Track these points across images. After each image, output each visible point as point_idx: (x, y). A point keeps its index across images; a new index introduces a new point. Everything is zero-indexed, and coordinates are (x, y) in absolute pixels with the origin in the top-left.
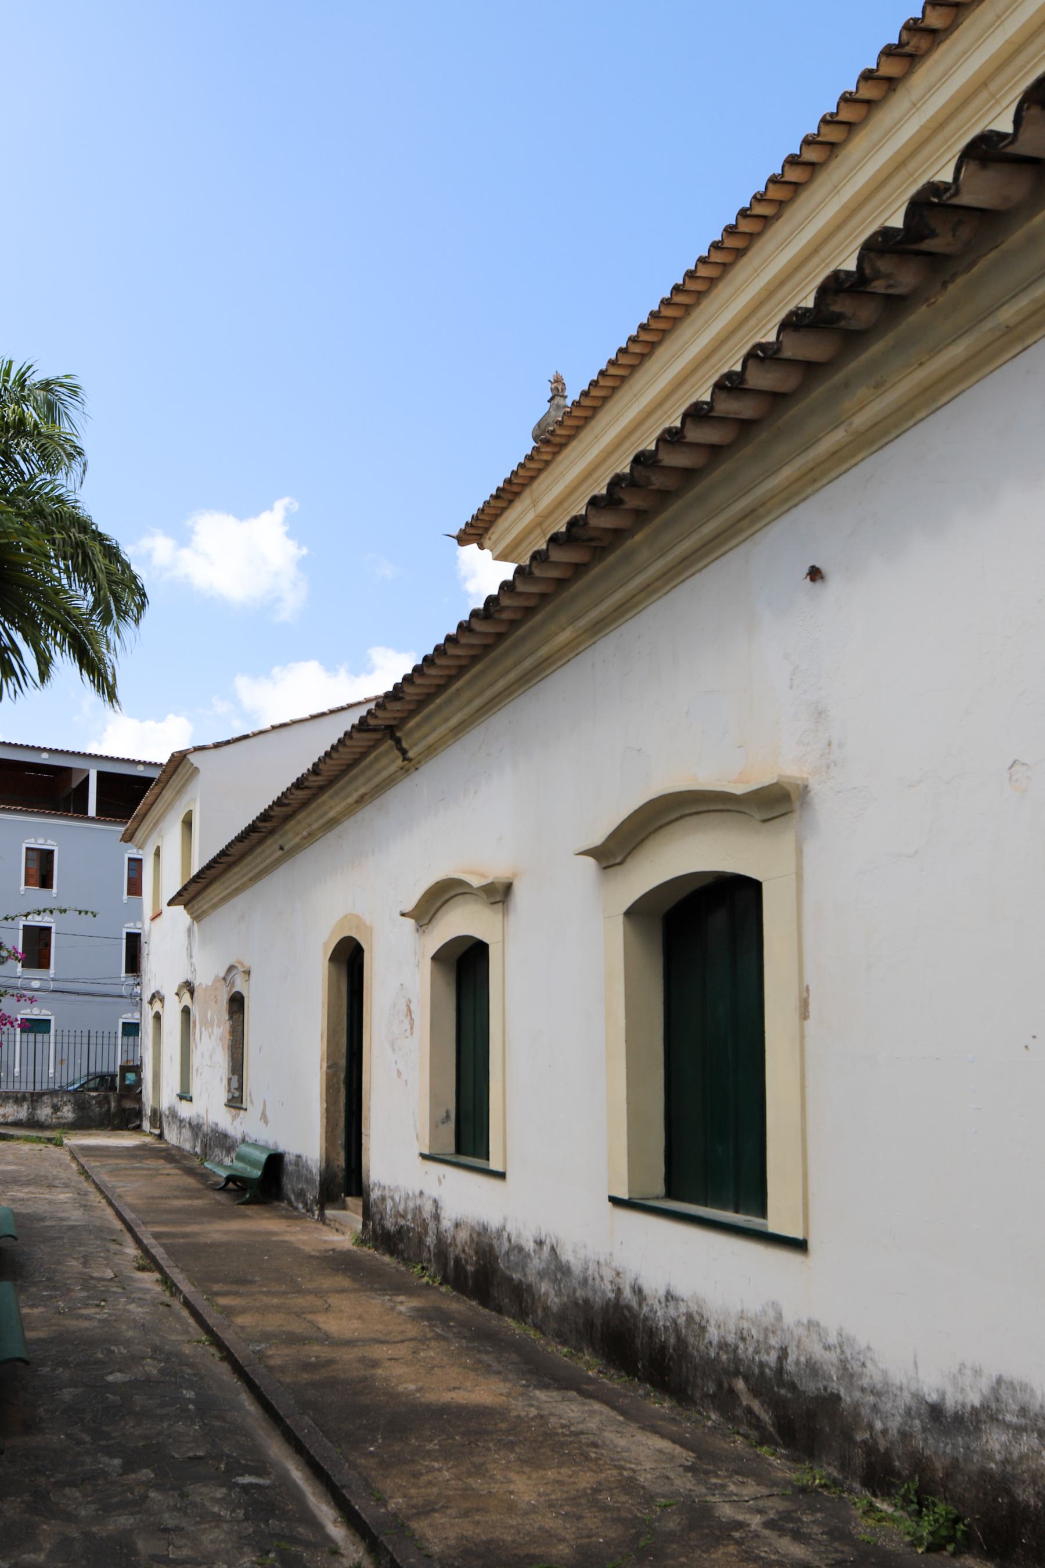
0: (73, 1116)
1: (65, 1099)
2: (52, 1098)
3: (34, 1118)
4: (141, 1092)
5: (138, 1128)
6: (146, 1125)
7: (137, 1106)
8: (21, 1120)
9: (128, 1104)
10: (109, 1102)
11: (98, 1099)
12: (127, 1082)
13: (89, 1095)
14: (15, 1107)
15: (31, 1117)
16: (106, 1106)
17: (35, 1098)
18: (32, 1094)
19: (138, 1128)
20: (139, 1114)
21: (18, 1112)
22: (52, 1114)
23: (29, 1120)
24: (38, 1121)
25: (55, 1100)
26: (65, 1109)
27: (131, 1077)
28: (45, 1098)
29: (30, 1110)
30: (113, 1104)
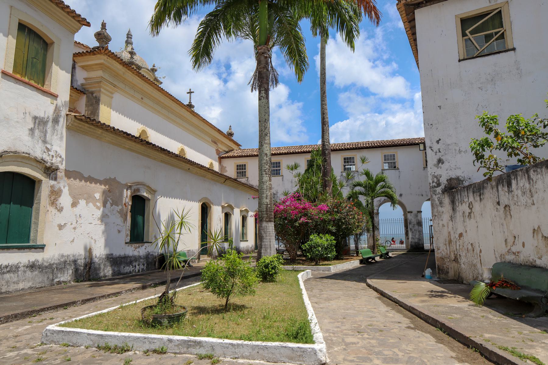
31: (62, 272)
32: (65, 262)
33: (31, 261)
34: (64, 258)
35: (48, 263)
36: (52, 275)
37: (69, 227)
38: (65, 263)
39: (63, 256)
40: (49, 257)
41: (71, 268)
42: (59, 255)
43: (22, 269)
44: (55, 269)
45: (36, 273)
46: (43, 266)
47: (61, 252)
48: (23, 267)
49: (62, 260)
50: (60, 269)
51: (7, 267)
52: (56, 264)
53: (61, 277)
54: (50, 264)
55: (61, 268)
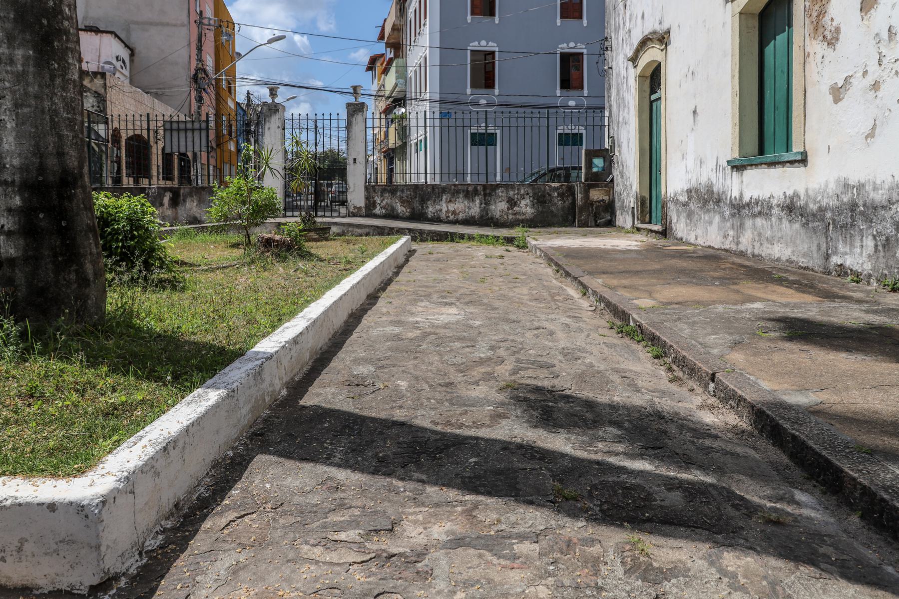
0: (533, 211)
1: (522, 192)
2: (507, 190)
3: (487, 214)
4: (612, 180)
5: (610, 223)
6: (624, 220)
7: (606, 198)
8: (473, 217)
9: (596, 195)
10: (573, 194)
11: (561, 191)
12: (595, 170)
13: (550, 186)
14: (466, 202)
15: (484, 213)
16: (570, 199)
17: (488, 191)
18: (485, 187)
19: (610, 223)
20: (609, 208)
21: (469, 208)
22: (508, 209)
23: (482, 216)
24: (492, 218)
25: (511, 193)
26: (523, 203)
27: (598, 162)
28: (500, 191)
29: (483, 205)
30: (579, 196)
31: (848, 240)
32: (853, 206)
33: (787, 194)
34: (850, 194)
35: (818, 205)
36: (824, 240)
37: (859, 84)
38: (852, 211)
39: (847, 186)
40: (817, 187)
41: (870, 231)
42: (838, 181)
43: (775, 211)
44: (831, 226)
45: (797, 226)
46: (808, 210)
47: (843, 175)
48: (778, 207)
49: (845, 200)
50: (841, 227)
51: (758, 203)
52: (832, 211)
53: (846, 254)
54: (821, 209)
55: (844, 226)
